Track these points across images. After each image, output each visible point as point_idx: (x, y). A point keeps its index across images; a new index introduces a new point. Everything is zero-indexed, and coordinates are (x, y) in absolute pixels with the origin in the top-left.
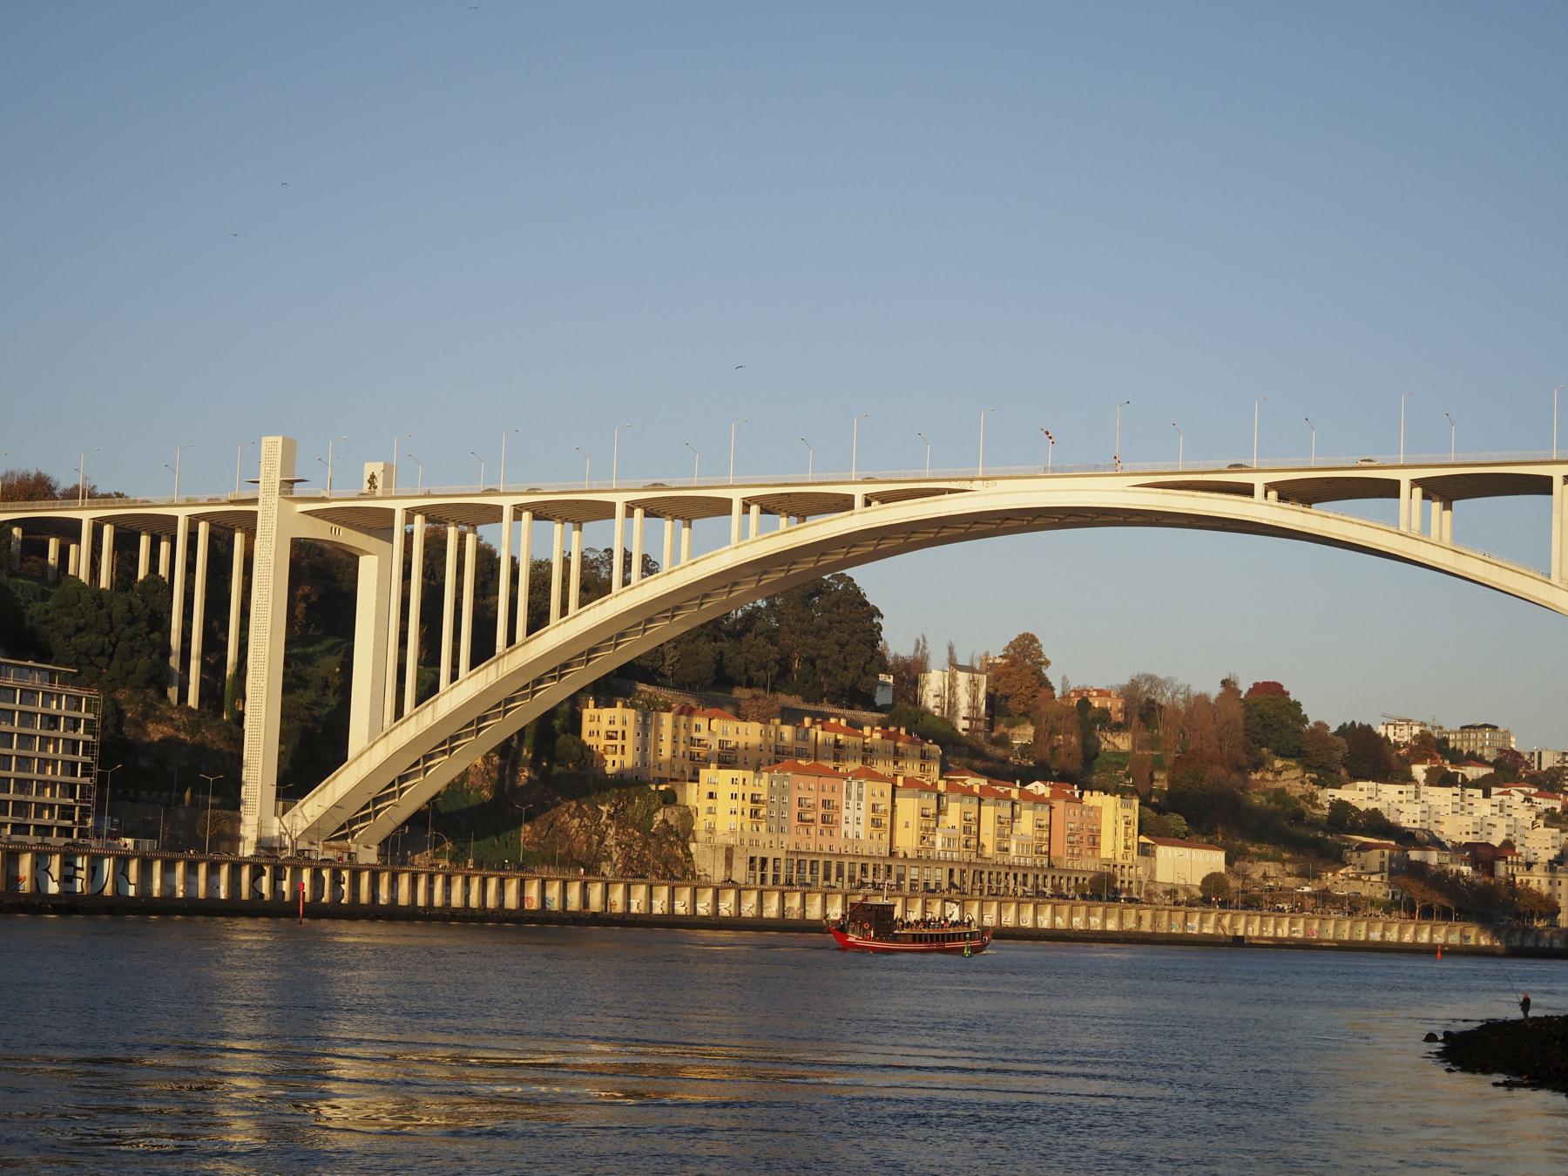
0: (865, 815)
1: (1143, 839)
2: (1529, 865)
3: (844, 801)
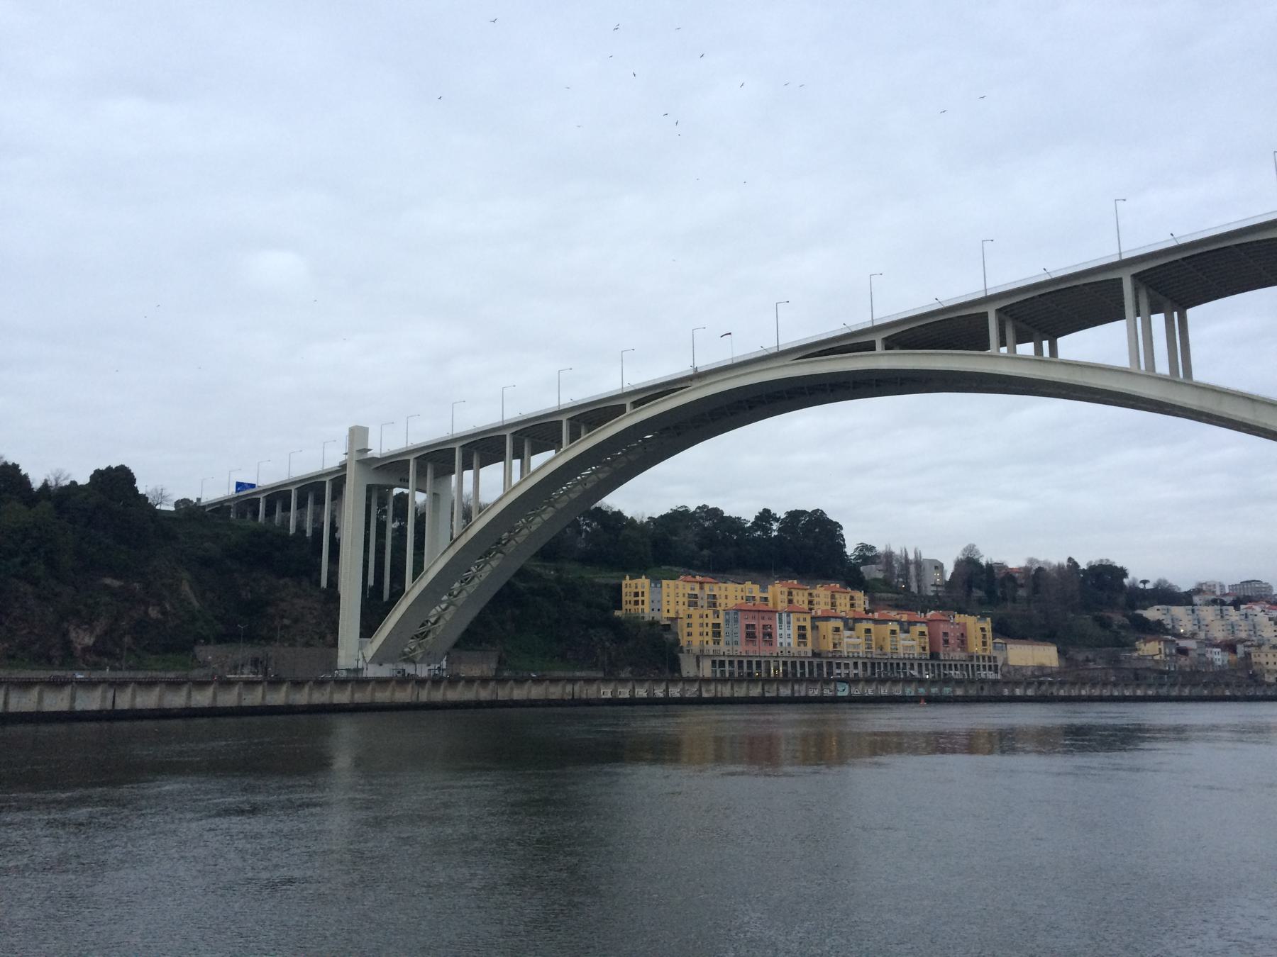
0: (793, 632)
1: (997, 640)
2: (1259, 646)
3: (778, 625)
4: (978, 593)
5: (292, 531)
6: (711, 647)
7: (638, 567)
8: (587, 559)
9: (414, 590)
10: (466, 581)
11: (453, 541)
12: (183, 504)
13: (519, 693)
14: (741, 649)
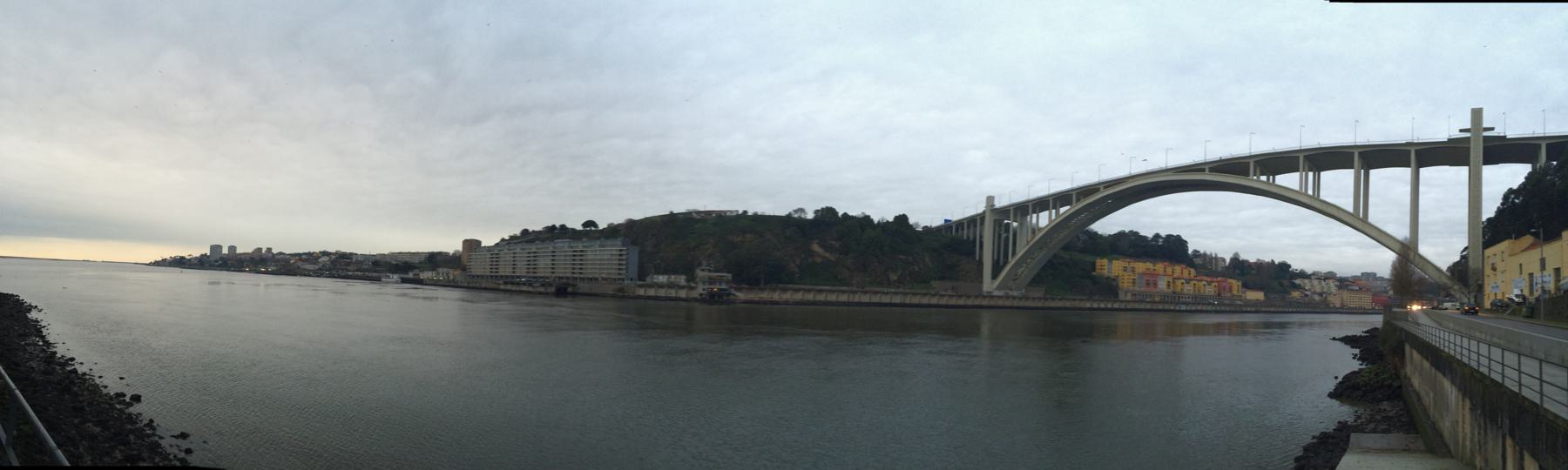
4: (1237, 271)
5: (965, 237)
6: (1131, 288)
7: (1103, 254)
8: (1083, 251)
9: (1012, 262)
10: (1034, 259)
11: (1028, 242)
12: (925, 228)
13: (1053, 304)
14: (1143, 289)
